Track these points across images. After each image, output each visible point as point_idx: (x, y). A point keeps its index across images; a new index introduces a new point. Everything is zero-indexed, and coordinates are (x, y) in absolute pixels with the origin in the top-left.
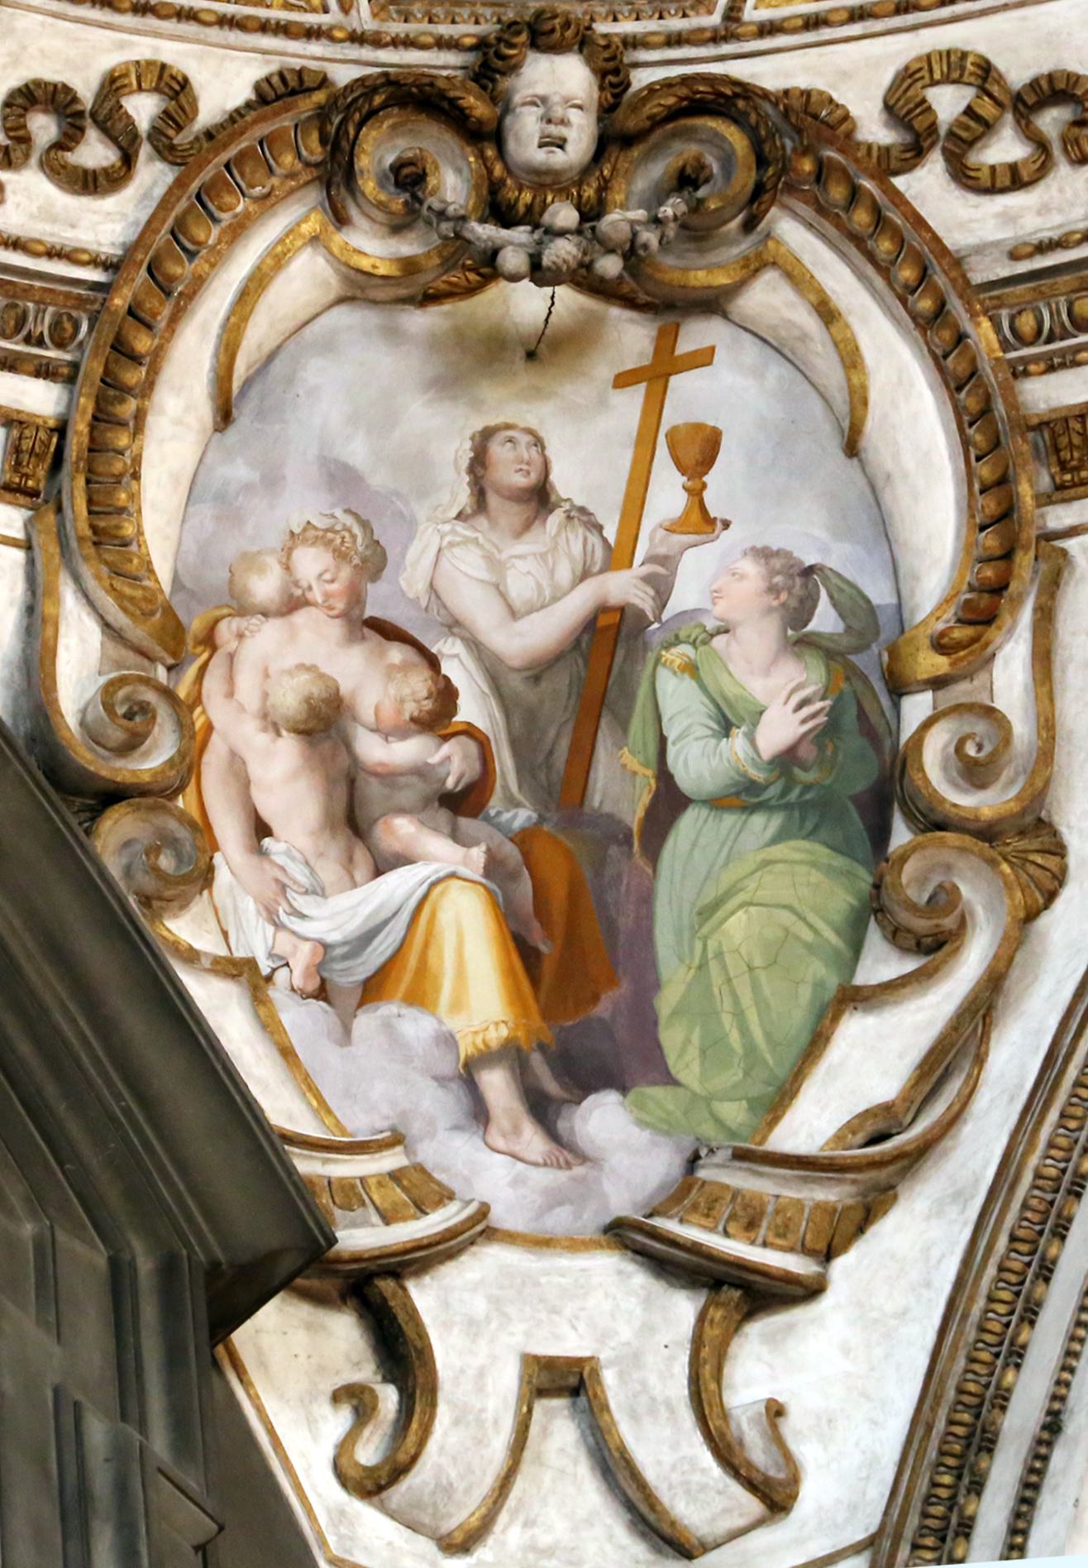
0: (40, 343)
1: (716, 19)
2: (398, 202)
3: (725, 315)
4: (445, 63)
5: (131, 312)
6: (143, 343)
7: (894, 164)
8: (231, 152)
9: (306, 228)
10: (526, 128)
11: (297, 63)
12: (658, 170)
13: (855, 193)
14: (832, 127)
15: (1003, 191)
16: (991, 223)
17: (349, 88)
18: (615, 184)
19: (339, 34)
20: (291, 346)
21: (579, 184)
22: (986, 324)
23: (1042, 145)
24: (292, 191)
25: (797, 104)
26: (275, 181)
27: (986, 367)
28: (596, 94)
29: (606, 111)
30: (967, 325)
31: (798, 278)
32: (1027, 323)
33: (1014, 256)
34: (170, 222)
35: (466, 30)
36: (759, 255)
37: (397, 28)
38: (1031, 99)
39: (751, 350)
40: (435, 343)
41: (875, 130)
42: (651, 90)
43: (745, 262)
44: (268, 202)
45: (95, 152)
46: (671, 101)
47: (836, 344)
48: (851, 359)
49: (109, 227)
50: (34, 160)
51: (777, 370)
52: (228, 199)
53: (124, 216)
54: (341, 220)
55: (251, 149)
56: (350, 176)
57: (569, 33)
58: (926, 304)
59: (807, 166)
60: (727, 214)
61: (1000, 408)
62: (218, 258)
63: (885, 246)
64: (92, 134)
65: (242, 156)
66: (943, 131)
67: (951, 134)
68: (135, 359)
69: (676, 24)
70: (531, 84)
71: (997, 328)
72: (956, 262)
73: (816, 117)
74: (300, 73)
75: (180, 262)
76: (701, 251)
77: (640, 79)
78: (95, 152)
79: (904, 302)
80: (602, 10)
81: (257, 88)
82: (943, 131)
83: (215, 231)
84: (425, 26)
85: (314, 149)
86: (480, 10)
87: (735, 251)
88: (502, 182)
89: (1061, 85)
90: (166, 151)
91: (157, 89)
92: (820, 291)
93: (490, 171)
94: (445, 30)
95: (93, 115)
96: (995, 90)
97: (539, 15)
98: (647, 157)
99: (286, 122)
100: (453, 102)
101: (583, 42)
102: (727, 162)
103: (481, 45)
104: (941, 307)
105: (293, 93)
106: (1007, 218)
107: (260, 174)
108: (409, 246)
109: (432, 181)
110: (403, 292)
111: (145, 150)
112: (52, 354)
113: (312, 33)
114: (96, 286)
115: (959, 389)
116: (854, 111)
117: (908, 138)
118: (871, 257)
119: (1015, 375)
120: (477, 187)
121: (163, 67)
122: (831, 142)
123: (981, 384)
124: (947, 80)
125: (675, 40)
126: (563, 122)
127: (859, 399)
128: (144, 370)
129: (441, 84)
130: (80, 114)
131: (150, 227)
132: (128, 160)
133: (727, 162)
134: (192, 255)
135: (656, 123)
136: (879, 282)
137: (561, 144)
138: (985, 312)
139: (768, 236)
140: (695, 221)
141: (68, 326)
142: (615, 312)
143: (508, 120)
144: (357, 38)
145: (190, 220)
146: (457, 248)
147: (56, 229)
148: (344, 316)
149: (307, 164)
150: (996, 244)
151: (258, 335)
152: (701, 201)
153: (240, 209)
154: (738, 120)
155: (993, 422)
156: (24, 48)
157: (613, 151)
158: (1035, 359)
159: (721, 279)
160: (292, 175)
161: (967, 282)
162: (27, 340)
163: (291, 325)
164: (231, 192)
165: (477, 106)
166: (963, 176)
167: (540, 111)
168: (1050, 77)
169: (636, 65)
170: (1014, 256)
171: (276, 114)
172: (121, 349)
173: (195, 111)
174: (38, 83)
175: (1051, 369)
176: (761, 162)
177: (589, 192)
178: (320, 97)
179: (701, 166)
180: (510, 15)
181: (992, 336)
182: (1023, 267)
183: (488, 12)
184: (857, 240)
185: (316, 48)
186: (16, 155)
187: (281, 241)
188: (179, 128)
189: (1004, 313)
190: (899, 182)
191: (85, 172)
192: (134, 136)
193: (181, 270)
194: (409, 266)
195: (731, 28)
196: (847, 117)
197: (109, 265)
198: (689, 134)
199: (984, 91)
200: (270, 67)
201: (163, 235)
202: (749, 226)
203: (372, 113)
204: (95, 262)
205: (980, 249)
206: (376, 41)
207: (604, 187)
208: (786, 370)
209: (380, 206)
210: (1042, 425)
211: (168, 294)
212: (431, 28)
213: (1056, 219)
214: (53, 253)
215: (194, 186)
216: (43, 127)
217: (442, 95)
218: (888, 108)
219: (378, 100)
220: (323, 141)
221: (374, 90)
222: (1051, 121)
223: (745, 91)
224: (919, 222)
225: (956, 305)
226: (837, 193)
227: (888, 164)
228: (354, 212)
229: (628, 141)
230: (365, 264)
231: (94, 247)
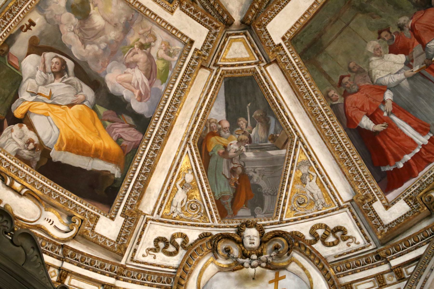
0: (165, 283)
1: (278, 220)
2: (226, 254)
3: (287, 270)
4: (232, 231)
5: (181, 277)
6: (183, 282)
7: (312, 243)
8: (196, 248)
9: (210, 260)
10: (247, 241)
11: (206, 232)
12: (270, 247)
13: (306, 248)
14: (301, 238)
15: (332, 246)
16: (331, 252)
17: (215, 236)
18: (264, 249)
19: (213, 226)
20: (211, 280)
21: (258, 249)
22: (331, 269)
23: (337, 238)
24: (207, 254)
25: (294, 234)
26: (204, 252)
27: (333, 277)
28: (259, 234)
29: (261, 237)
30: (328, 270)
31: (298, 263)
32: (339, 268)
33: (335, 257)
34: (186, 260)
35: (235, 224)
36: (291, 260)
37: (223, 225)
38: (334, 231)
39: (292, 276)
40: (236, 278)
41: (308, 237)
42: (268, 234)
43: (288, 261)
44: (203, 256)
45: (171, 249)
46: (271, 235)
47: (306, 274)
48: (309, 277)
49: (175, 262)
50: (160, 251)
51: (297, 279)
52: (195, 256)
53: (178, 259)
54: (216, 258)
55: (199, 247)
56: (217, 251)
57: (252, 225)
58: (321, 267)
59: (297, 244)
60: (284, 253)
61: (336, 283)
62: (195, 266)
63: (312, 257)
64: (170, 246)
65: (197, 249)
66: (320, 237)
67: (321, 237)
68: (182, 285)
69: (272, 221)
70: (247, 233)
71: (334, 270)
72: (325, 259)
73: (298, 236)
74: (206, 233)
75: (188, 268)
76: (281, 259)
77: (267, 231)
78: (171, 249)
79: (317, 266)
80: (259, 219)
81: (199, 236)
82: (320, 237)
83: (194, 262)
84: (228, 224)
85: (210, 247)
86: (237, 221)
87: (287, 259)
88: (244, 250)
89: (339, 228)
90: (184, 248)
91: (181, 237)
92: (302, 265)
93: (242, 249)
94: (231, 225)
95: (170, 242)
96: (328, 230)
97: (247, 221)
98: (269, 244)
99: (205, 242)
100: (233, 238)
101: (255, 225)
102: (283, 244)
103: (238, 227)
104: (323, 267)
105: (206, 237)
106: (333, 251)
107: (201, 251)
108: (229, 262)
109: (231, 251)
110: (229, 270)
111: (180, 248)
112: (167, 285)
113: (208, 226)
114: (174, 272)
115: (328, 280)
116: (304, 234)
117: (314, 238)
118: (310, 259)
119: (338, 277)
120: (240, 251)
121: (182, 233)
122: (301, 240)
123: (332, 280)
124: (319, 228)
125: (272, 224)
126: (253, 240)
127: (311, 283)
128: (184, 287)
129: (231, 235)
130: (168, 242)
131: (182, 262)
132: (177, 250)
133: (283, 244)
134: (190, 266)
135: (269, 239)
136: (312, 263)
137: (254, 243)
138: (331, 267)
139: (292, 256)
140: (278, 255)
141: (169, 280)
142: (267, 270)
143: (244, 240)
144: (216, 227)
145: (189, 260)
146: (237, 263)
147: (166, 263)
148: (219, 274)
149: (209, 249)
150: (332, 255)
151: (204, 279)
152: (279, 252)
153: (198, 258)
154: (284, 238)
155: (335, 286)
156: (156, 231)
157: (263, 244)
158: (341, 274)
159: (285, 264)
160: (206, 251)
161: (327, 263)
162: (163, 283)
163: (210, 277)
164: (196, 255)
165: (238, 238)
166: (324, 244)
167: (249, 238)
168: (337, 227)
169: (266, 229)
170: (335, 257)
171: (203, 241)
172: (179, 284)
173: (189, 241)
174: (160, 237)
175: (344, 276)
176: (289, 244)
177: (260, 251)
178: (210, 237)
179: (278, 246)
180: (243, 221)
181: (333, 271)
182: (337, 259)
183: (239, 221)
184: (307, 256)
185: (209, 229)
186: (157, 250)
187: (206, 263)
188: (186, 244)
189: (335, 267)
190: (313, 246)
191: (170, 252)
192: (178, 246)
193: (189, 269)
194: (230, 265)
195: (281, 222)
196: (303, 235)
197: (176, 269)
198: (276, 240)
199: (326, 230)
200: (201, 232)
201: (185, 263)
202: (288, 255)
203: (219, 240)
204: (173, 268)
205: (329, 256)
206: (219, 227)
207: (262, 250)
208: (298, 279)
209: (223, 256)
210: (344, 285)
211: (187, 273)
212: (229, 224)
213: (342, 250)
214: (166, 267)
215: (189, 254)
216: (161, 245)
217: (231, 236)
218: (310, 233)
219: (220, 238)
220: (211, 245)
221: (219, 236)
222: (338, 234)
223: (285, 233)
224: (318, 253)
225: (326, 267)
226: (303, 249)
227: (311, 243)
228: (219, 257)
229: (265, 242)
230: (222, 266)
231: (173, 265)
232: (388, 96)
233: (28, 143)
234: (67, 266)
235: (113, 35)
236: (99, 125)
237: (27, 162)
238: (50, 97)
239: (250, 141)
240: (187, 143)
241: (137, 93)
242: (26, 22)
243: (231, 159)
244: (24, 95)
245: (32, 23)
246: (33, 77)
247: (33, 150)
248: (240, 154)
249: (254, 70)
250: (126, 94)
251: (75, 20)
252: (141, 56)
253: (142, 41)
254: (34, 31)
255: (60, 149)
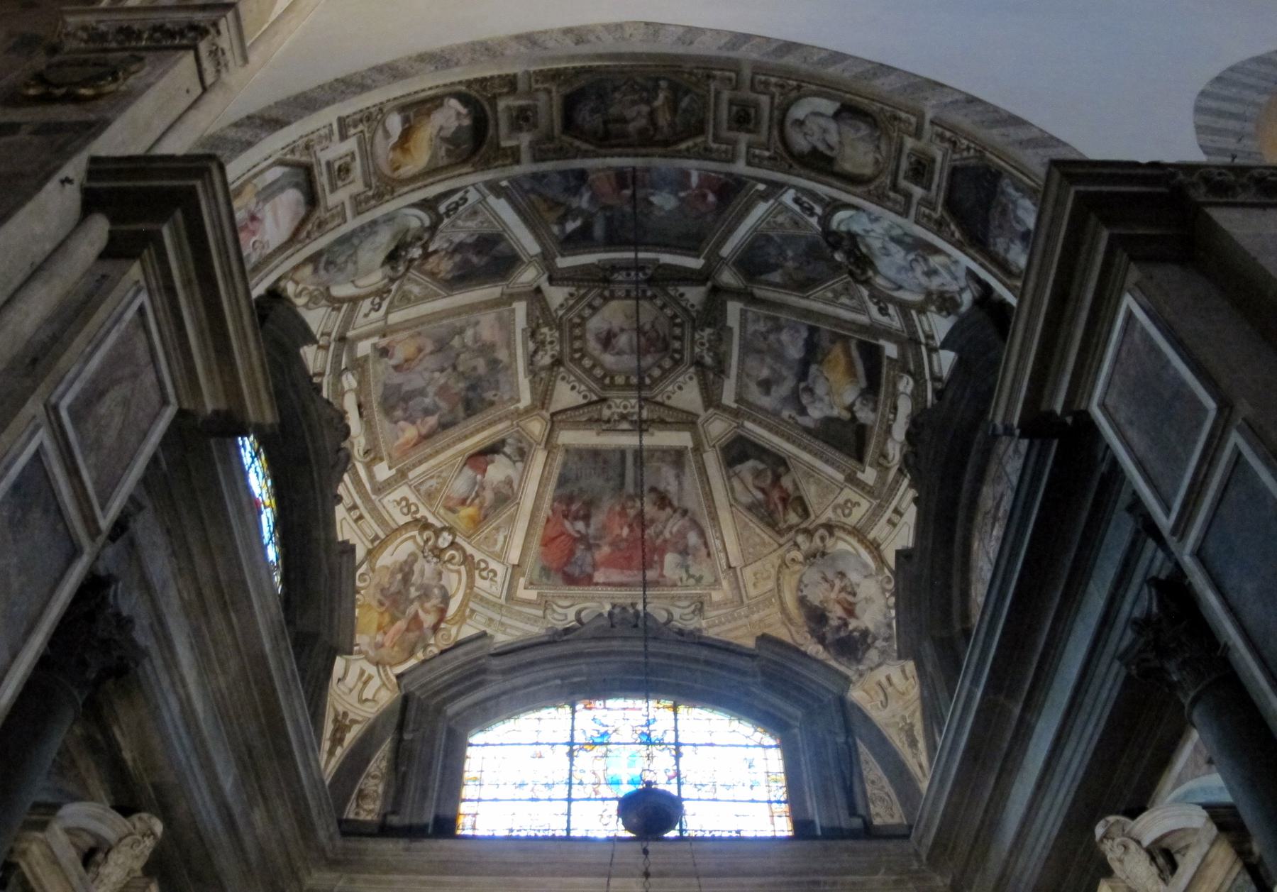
232: (682, 194)
233: (864, 405)
234: (927, 376)
235: (768, 360)
236: (830, 357)
237: (876, 403)
238: (828, 394)
239: (780, 254)
240: (808, 298)
241: (796, 335)
242: (791, 421)
243: (801, 264)
244: (835, 412)
245: (790, 417)
246: (821, 409)
247: (867, 400)
248: (793, 259)
249: (734, 264)
250: (801, 343)
251: (774, 389)
252: (772, 337)
253: (762, 339)
254: (794, 414)
255: (858, 382)
